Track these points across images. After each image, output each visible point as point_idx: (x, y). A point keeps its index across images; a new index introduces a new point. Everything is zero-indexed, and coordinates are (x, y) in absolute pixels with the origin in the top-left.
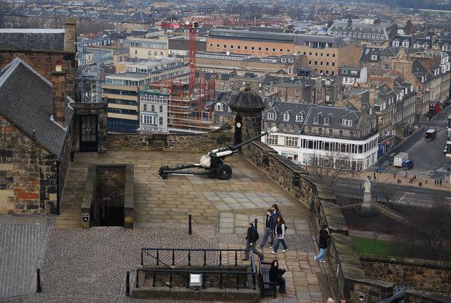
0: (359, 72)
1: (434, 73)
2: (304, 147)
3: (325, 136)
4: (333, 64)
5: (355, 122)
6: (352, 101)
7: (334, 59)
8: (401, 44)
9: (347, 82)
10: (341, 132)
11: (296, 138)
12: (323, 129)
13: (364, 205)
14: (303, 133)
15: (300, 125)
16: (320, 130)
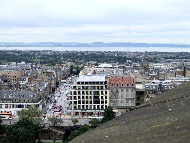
0: (25, 79)
1: (52, 77)
2: (14, 108)
3: (22, 102)
4: (15, 77)
5: (34, 96)
6: (30, 88)
7: (15, 75)
8: (35, 69)
9: (21, 83)
10: (28, 100)
11: (10, 105)
12: (21, 100)
13: (45, 128)
14: (13, 102)
15: (11, 99)
16: (20, 100)
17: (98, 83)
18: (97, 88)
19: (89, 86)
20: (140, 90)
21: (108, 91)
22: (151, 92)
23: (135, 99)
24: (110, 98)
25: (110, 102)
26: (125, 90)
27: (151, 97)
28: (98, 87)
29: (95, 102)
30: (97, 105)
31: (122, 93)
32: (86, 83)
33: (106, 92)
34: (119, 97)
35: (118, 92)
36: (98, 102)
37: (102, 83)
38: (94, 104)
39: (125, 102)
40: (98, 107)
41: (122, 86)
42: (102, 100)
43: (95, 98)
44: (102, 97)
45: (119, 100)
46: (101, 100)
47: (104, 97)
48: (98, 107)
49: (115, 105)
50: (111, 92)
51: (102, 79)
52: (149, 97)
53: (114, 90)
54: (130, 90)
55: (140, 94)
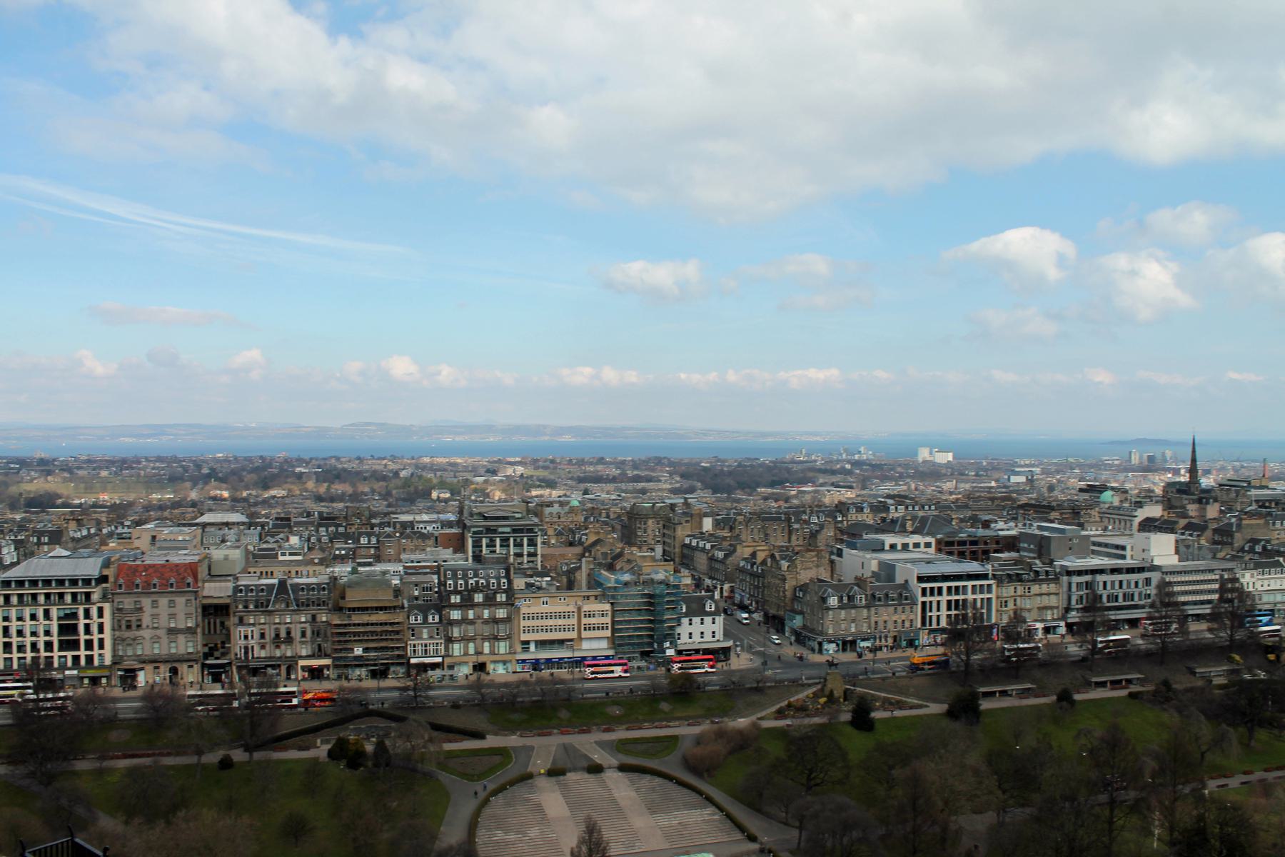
17: (74, 582)
18: (68, 598)
19: (41, 591)
20: (216, 601)
21: (107, 607)
22: (251, 607)
23: (199, 630)
24: (113, 629)
25: (116, 641)
26: (163, 601)
27: (252, 621)
28: (74, 595)
29: (64, 646)
30: (69, 654)
31: (155, 611)
32: (34, 583)
33: (100, 611)
34: (144, 626)
35: (140, 609)
36: (74, 645)
37: (87, 582)
38: (60, 649)
39: (165, 640)
40: (76, 658)
41: (148, 589)
42: (88, 637)
43: (63, 629)
44: (87, 627)
45: (146, 633)
46: (83, 637)
47: (95, 629)
48: (76, 658)
49: (130, 653)
50: (117, 611)
51: (90, 566)
52: (245, 621)
53: (128, 603)
54: (181, 600)
55: (215, 612)
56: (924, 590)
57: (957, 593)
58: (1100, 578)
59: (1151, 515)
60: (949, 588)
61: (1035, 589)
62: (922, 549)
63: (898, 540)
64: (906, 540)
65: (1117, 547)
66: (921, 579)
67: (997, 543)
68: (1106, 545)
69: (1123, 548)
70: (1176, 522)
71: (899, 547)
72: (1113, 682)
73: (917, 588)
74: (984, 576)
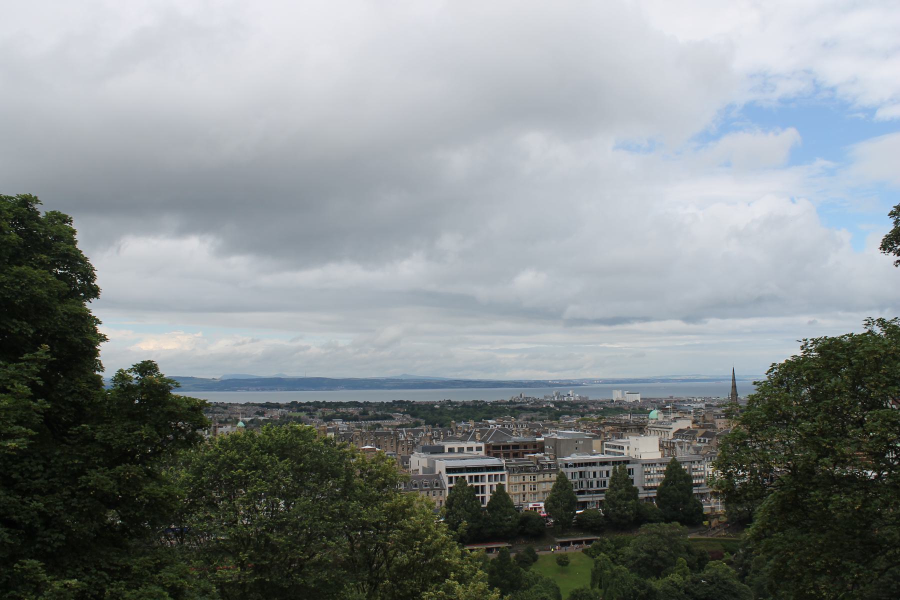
56: (451, 479)
57: (477, 481)
58: (591, 469)
59: (682, 428)
60: (471, 477)
61: (540, 478)
62: (475, 452)
63: (456, 445)
64: (462, 445)
65: (619, 447)
66: (449, 470)
67: (535, 447)
68: (614, 447)
69: (623, 448)
70: (696, 432)
71: (456, 451)
72: (575, 543)
73: (445, 477)
74: (500, 468)
